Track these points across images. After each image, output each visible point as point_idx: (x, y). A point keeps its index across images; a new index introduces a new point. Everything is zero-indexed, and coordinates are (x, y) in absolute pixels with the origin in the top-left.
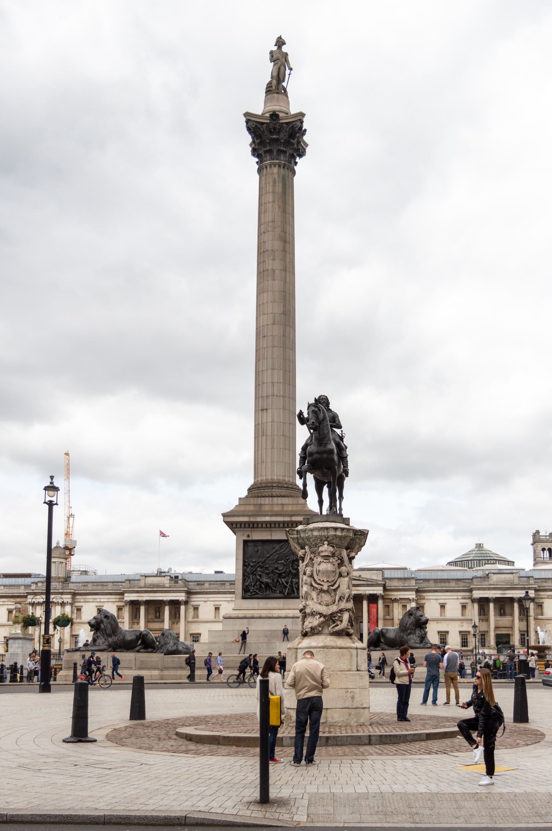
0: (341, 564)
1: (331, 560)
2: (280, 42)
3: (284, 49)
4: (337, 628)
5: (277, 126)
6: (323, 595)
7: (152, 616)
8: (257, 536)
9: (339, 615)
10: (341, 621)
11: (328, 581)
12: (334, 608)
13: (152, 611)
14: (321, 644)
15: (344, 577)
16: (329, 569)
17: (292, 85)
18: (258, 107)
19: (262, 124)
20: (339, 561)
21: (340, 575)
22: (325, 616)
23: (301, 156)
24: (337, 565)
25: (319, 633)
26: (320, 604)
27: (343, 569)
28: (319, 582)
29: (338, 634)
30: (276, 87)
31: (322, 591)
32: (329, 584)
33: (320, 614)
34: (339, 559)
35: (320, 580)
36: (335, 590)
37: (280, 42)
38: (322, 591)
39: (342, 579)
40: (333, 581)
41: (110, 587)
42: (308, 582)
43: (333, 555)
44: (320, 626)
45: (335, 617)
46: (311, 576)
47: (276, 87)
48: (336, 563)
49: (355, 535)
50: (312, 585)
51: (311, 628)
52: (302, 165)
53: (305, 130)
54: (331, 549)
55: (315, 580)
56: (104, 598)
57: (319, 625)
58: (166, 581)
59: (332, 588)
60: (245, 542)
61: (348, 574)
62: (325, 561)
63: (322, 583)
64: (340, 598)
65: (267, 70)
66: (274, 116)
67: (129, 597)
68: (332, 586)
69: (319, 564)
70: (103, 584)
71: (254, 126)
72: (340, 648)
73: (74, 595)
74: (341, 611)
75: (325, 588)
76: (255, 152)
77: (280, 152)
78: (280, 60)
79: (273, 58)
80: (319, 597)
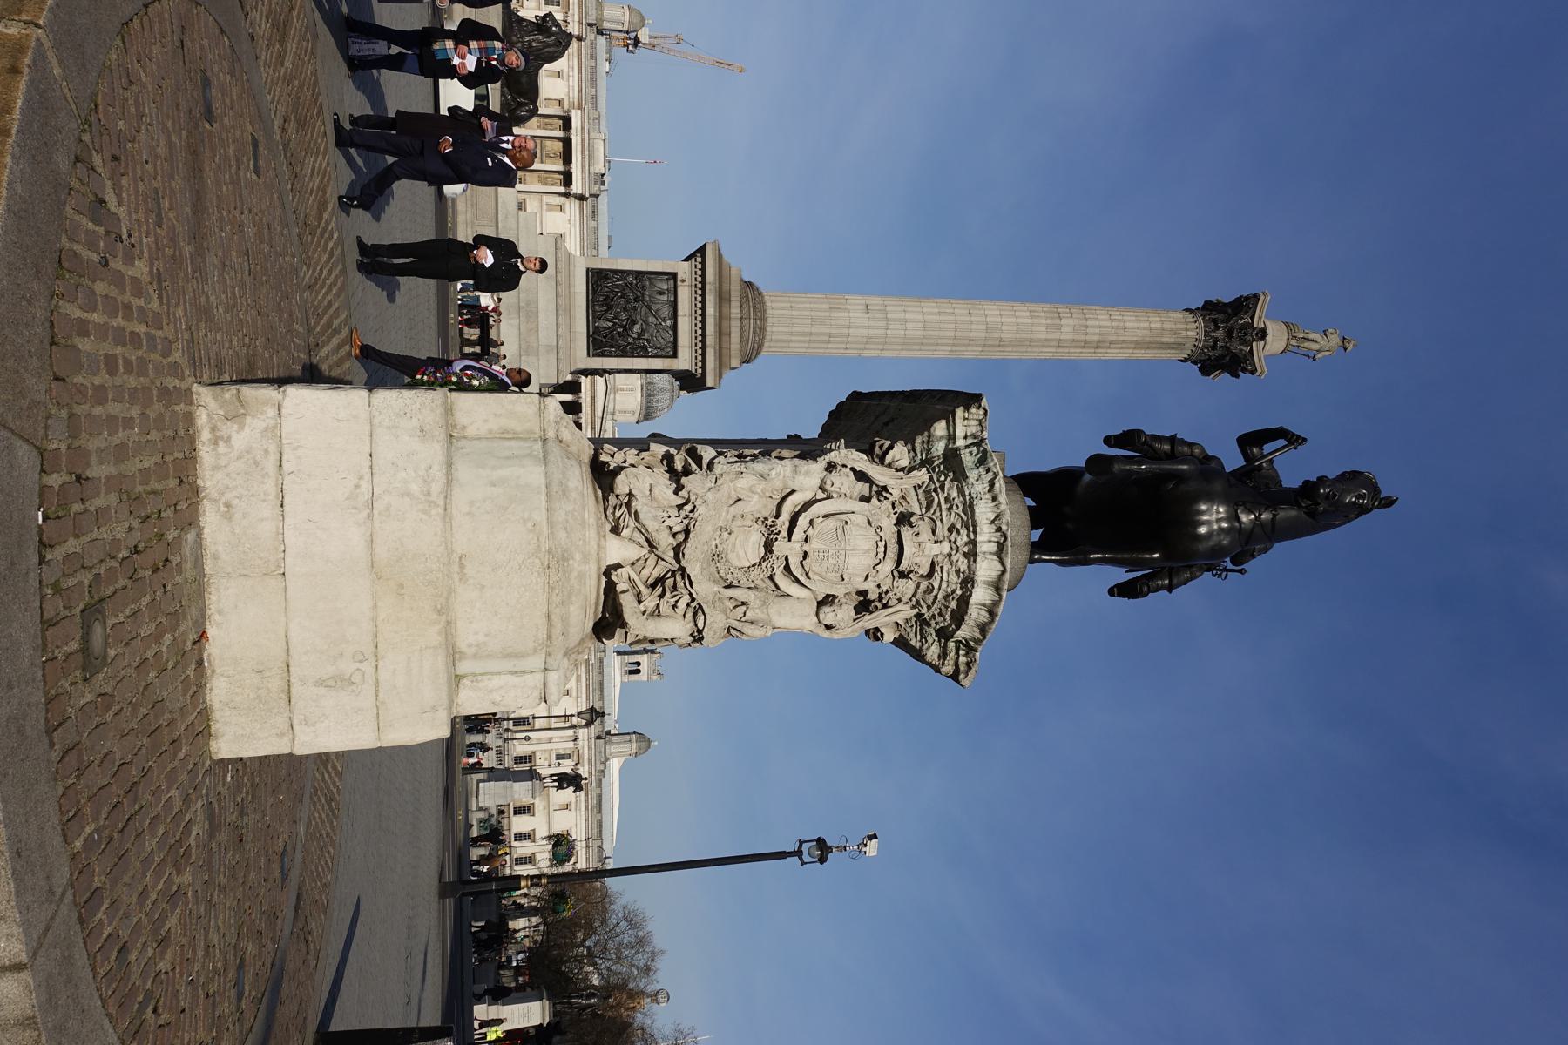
1: (888, 566)
5: (1249, 338)
6: (756, 538)
11: (806, 555)
15: (817, 615)
19: (1252, 318)
22: (678, 551)
23: (1201, 369)
24: (863, 587)
33: (687, 532)
48: (870, 586)
49: (958, 642)
53: (1238, 376)
55: (807, 506)
59: (779, 571)
61: (828, 627)
63: (798, 534)
75: (781, 547)
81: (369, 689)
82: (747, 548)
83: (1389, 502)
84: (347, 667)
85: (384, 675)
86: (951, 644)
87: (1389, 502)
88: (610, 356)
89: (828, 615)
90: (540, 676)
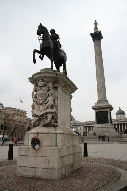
0: (49, 90)
1: (43, 88)
2: (96, 21)
3: (97, 22)
4: (44, 123)
6: (41, 106)
7: (89, 129)
8: (99, 111)
9: (46, 115)
10: (47, 119)
12: (43, 112)
13: (89, 128)
14: (35, 132)
16: (42, 93)
17: (98, 27)
18: (93, 32)
20: (48, 89)
21: (49, 96)
22: (39, 117)
23: (102, 38)
25: (38, 125)
26: (38, 111)
27: (49, 92)
28: (39, 100)
29: (47, 125)
30: (96, 28)
31: (40, 104)
32: (43, 100)
33: (37, 115)
34: (47, 87)
35: (39, 99)
36: (46, 103)
37: (96, 21)
38: (40, 104)
39: (49, 98)
40: (45, 99)
41: (82, 124)
42: (34, 101)
43: (45, 86)
44: (37, 122)
45: (44, 117)
46: (36, 98)
47: (96, 28)
49: (57, 76)
50: (37, 102)
51: (34, 123)
52: (102, 40)
54: (43, 83)
56: (81, 126)
57: (36, 121)
58: (91, 123)
59: (44, 102)
60: (97, 112)
61: (52, 95)
62: (40, 89)
64: (48, 107)
65: (94, 26)
66: (95, 32)
67: (85, 126)
68: (45, 101)
69: (38, 91)
70: (81, 123)
71: (92, 35)
72: (45, 134)
73: (76, 126)
74: (47, 113)
76: (93, 40)
77: (97, 38)
78: (96, 24)
79: (95, 24)
80: (39, 107)
81: (50, 158)
82: (42, 107)
83: (41, 24)
84: (47, 161)
85: (48, 156)
86: (57, 76)
87: (41, 24)
88: (108, 120)
89: (50, 95)
90: (57, 134)
